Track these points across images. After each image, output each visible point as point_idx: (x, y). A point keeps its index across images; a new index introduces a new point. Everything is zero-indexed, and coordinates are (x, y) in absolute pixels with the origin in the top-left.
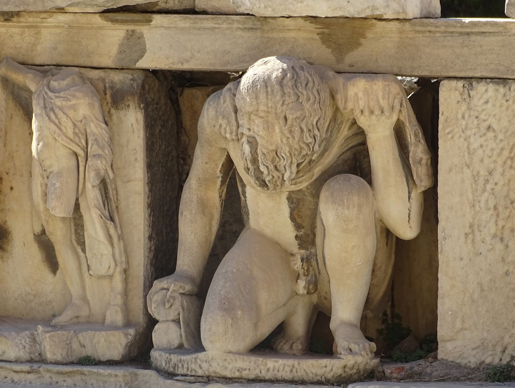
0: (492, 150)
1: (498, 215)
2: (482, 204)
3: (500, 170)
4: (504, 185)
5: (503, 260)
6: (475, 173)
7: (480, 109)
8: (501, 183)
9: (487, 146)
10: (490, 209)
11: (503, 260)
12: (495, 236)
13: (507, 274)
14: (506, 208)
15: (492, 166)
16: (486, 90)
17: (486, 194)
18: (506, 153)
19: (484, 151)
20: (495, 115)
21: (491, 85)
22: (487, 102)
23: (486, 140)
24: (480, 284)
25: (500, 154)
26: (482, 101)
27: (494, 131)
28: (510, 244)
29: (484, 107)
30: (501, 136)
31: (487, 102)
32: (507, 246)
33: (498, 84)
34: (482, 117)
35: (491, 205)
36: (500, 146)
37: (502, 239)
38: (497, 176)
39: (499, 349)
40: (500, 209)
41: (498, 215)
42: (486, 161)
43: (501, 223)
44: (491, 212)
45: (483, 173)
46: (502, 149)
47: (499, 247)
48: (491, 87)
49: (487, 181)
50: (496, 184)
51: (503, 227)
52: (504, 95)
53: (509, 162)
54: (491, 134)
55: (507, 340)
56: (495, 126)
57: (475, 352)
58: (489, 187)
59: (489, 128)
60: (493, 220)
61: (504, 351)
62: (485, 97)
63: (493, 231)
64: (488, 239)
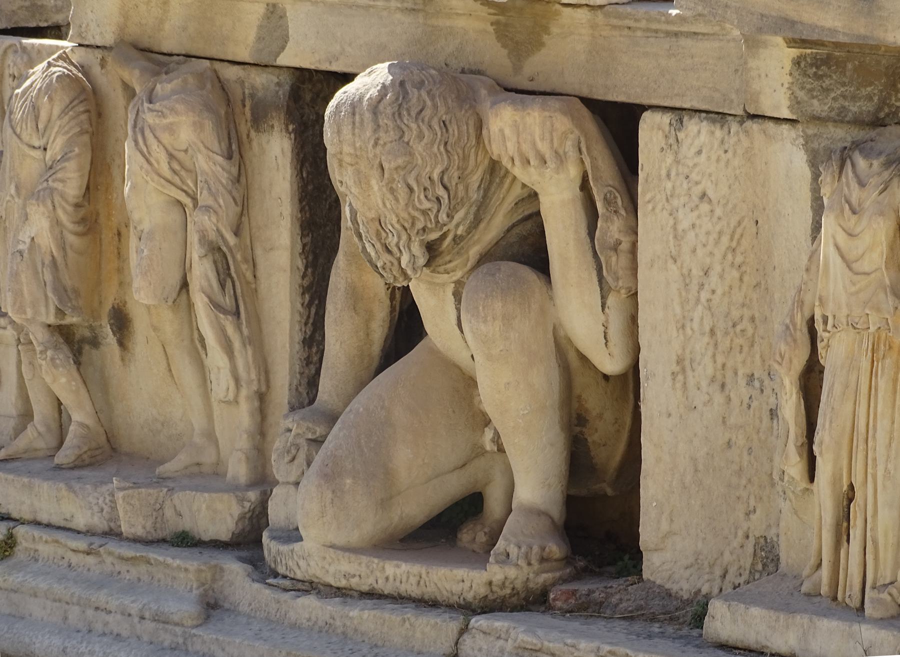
2: (696, 325)
3: (717, 268)
4: (724, 294)
6: (685, 271)
7: (691, 164)
8: (719, 292)
9: (701, 226)
10: (703, 334)
11: (724, 422)
13: (729, 444)
14: (727, 333)
15: (708, 260)
16: (699, 132)
17: (700, 307)
19: (697, 235)
20: (710, 175)
21: (705, 123)
22: (699, 152)
23: (699, 217)
24: (694, 460)
25: (717, 242)
26: (693, 150)
28: (732, 395)
29: (696, 160)
30: (719, 212)
31: (699, 152)
32: (729, 399)
33: (714, 122)
34: (694, 176)
35: (707, 329)
36: (718, 228)
38: (714, 278)
39: (718, 572)
40: (719, 334)
42: (700, 252)
43: (720, 359)
44: (706, 339)
45: (696, 272)
46: (720, 233)
47: (719, 398)
48: (705, 126)
52: (722, 142)
53: (730, 256)
54: (705, 207)
55: (727, 557)
56: (710, 193)
57: (688, 572)
58: (704, 295)
59: (704, 195)
60: (710, 353)
61: (724, 577)
62: (697, 143)
63: (710, 371)
64: (704, 384)
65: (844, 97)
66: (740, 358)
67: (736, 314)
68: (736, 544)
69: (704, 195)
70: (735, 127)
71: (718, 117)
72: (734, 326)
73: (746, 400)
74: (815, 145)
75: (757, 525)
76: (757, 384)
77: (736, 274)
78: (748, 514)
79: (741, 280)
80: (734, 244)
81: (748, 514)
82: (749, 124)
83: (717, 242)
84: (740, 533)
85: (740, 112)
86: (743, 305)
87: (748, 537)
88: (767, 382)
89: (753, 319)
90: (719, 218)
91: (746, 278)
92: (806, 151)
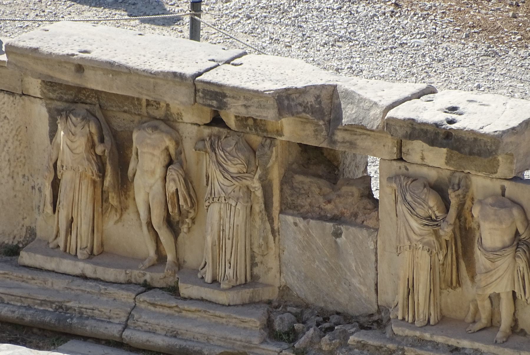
0: (7, 129)
1: (10, 164)
3: (11, 140)
5: (13, 189)
8: (12, 148)
12: (9, 175)
13: (15, 196)
14: (15, 161)
15: (7, 138)
16: (4, 97)
17: (4, 153)
18: (14, 132)
21: (6, 95)
22: (4, 103)
25: (11, 132)
27: (8, 119)
28: (17, 181)
29: (3, 106)
30: (11, 123)
31: (4, 103)
32: (15, 182)
33: (10, 94)
35: (7, 159)
36: (11, 128)
37: (13, 177)
38: (10, 144)
39: (12, 237)
40: (12, 162)
41: (10, 164)
42: (4, 135)
43: (12, 169)
44: (7, 163)
46: (12, 130)
47: (11, 181)
49: (5, 146)
50: (9, 148)
51: (13, 171)
52: (13, 101)
54: (6, 121)
56: (8, 116)
58: (6, 149)
59: (5, 117)
60: (8, 167)
62: (3, 101)
63: (8, 172)
64: (6, 176)
65: (61, 93)
66: (20, 169)
67: (18, 155)
68: (19, 228)
69: (5, 117)
70: (18, 97)
71: (12, 94)
72: (18, 159)
73: (22, 182)
74: (50, 106)
75: (27, 222)
76: (26, 178)
77: (18, 143)
78: (23, 219)
79: (20, 145)
80: (17, 133)
81: (23, 219)
82: (24, 97)
83: (11, 132)
84: (21, 225)
85: (21, 93)
86: (21, 153)
87: (23, 226)
88: (30, 177)
89: (25, 157)
90: (12, 125)
91: (22, 145)
92: (47, 108)
